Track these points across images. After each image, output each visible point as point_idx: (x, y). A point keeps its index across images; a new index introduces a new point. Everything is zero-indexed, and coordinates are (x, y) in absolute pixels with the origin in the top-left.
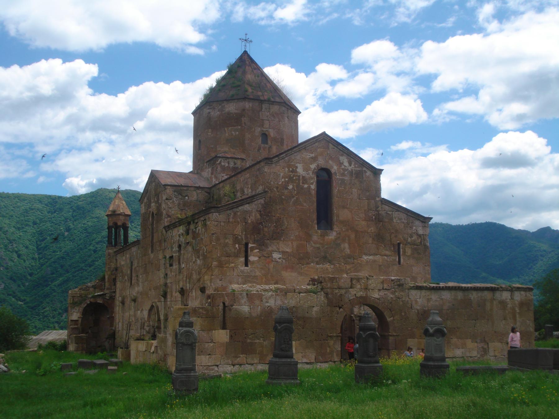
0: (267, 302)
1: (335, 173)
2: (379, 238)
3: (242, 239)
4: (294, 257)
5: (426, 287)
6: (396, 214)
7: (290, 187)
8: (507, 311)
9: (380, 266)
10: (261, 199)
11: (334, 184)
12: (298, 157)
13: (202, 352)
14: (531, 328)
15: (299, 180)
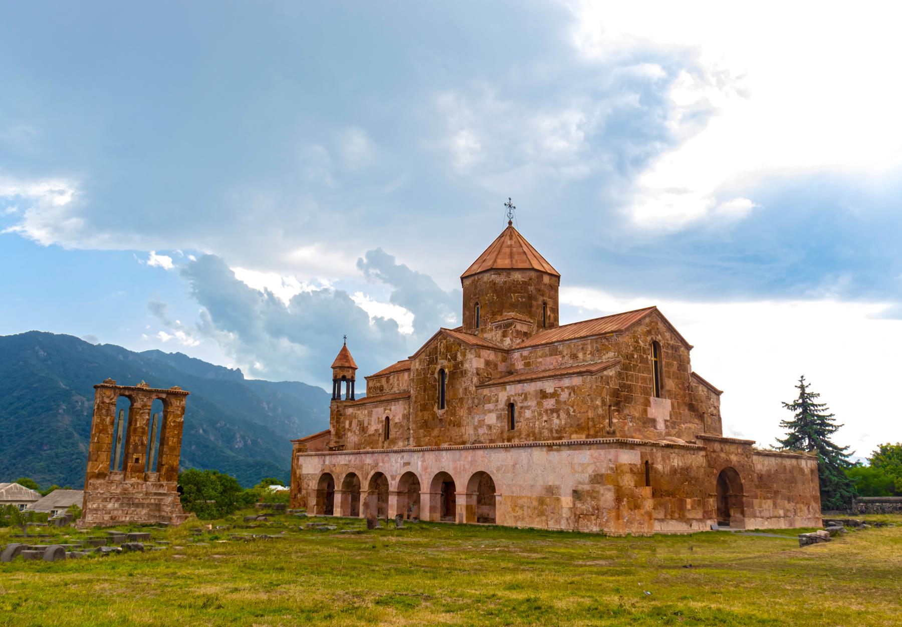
2: (692, 407)
6: (701, 388)
7: (635, 356)
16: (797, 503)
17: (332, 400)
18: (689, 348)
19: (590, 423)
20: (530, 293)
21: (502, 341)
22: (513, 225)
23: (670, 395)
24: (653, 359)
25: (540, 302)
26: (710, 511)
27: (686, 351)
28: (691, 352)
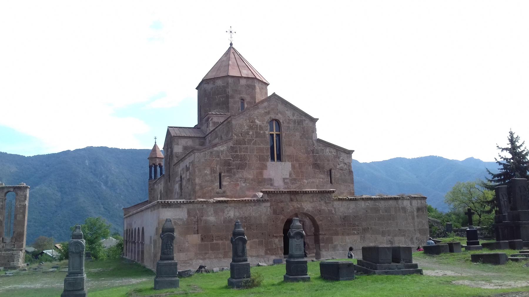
0: (228, 214)
1: (283, 122)
2: (316, 166)
3: (217, 170)
4: (255, 181)
5: (346, 199)
6: (328, 150)
7: (251, 133)
8: (407, 214)
9: (317, 185)
10: (230, 142)
11: (283, 130)
12: (256, 112)
13: (180, 251)
14: (426, 226)
15: (257, 128)
16: (396, 236)
17: (149, 179)
18: (314, 120)
19: (197, 187)
20: (228, 94)
21: (207, 130)
22: (233, 46)
23: (291, 158)
24: (275, 133)
25: (237, 98)
26: (275, 249)
27: (311, 124)
28: (317, 124)
